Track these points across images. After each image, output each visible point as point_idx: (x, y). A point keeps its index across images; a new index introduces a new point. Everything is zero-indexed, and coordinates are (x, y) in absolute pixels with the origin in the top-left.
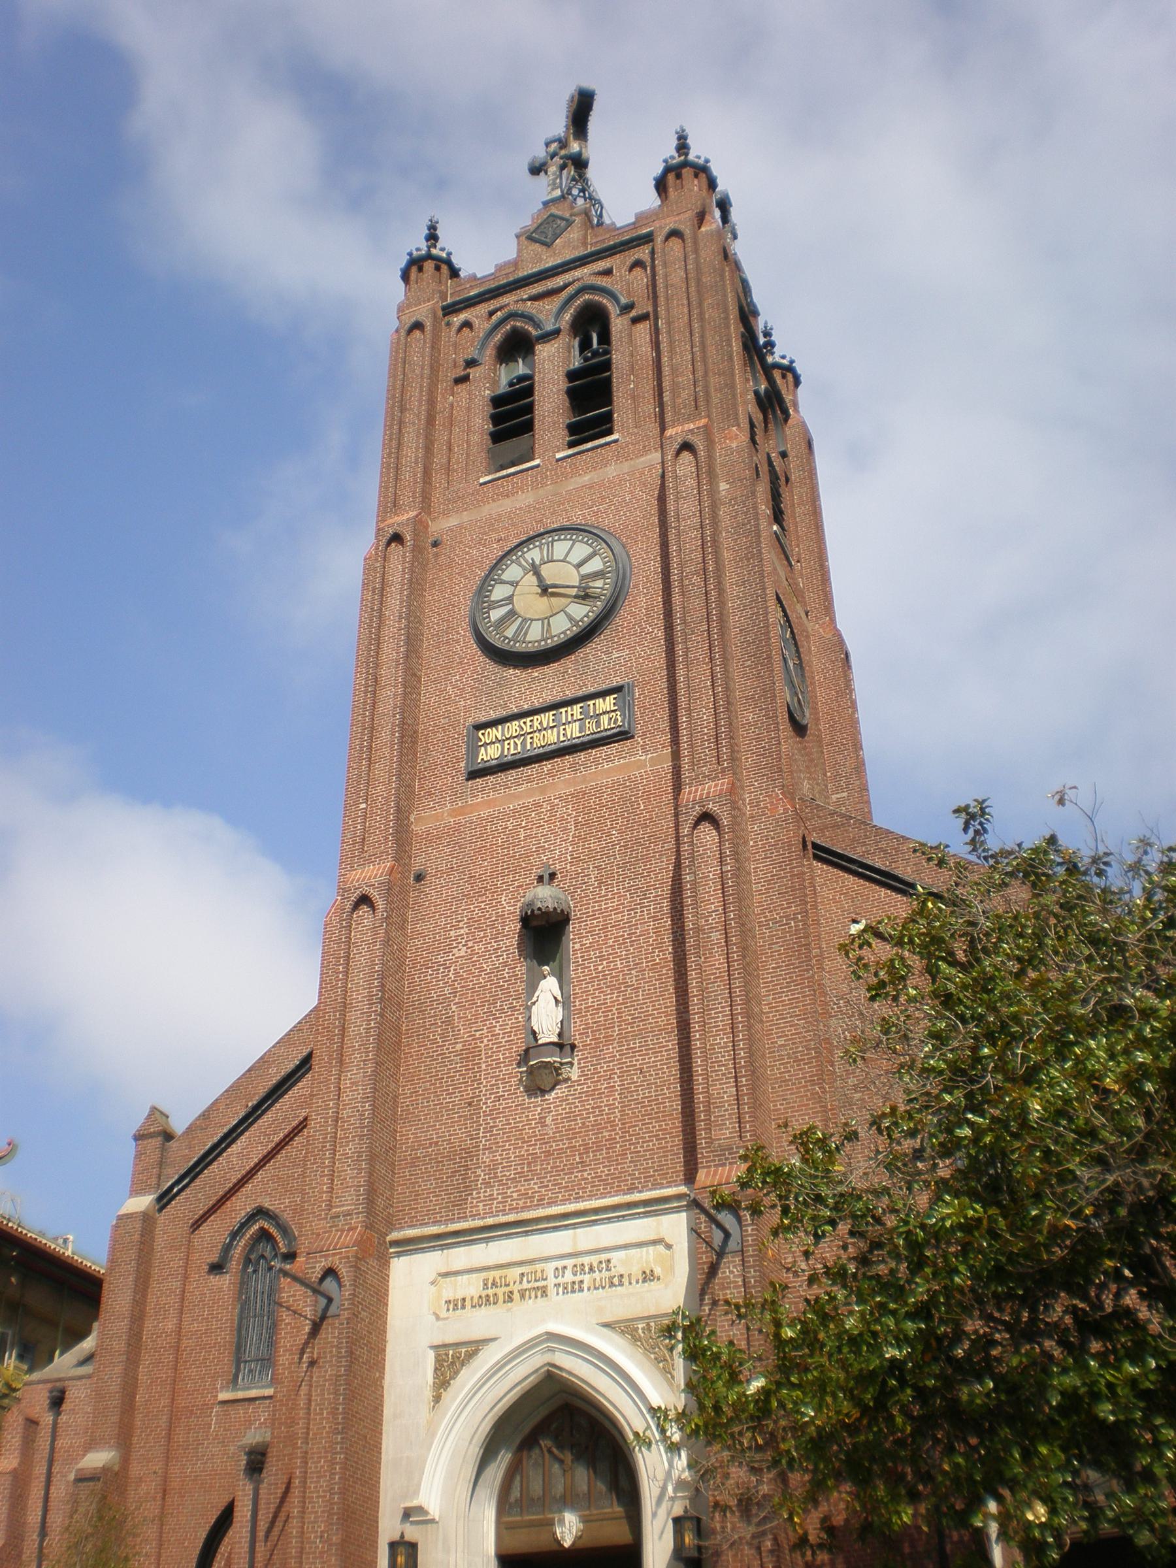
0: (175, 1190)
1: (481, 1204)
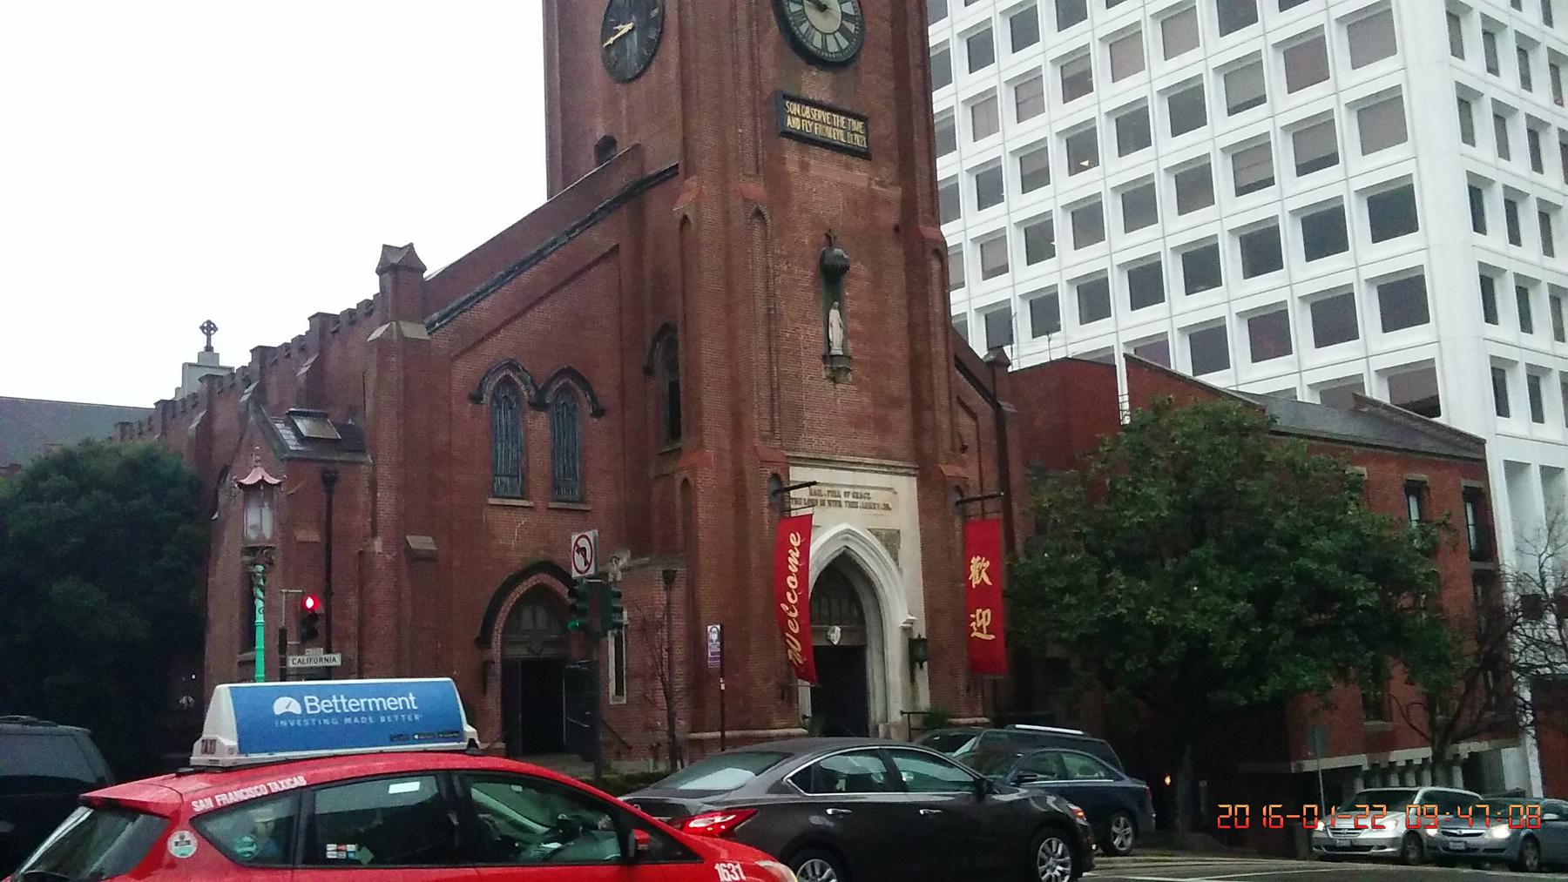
0: (437, 325)
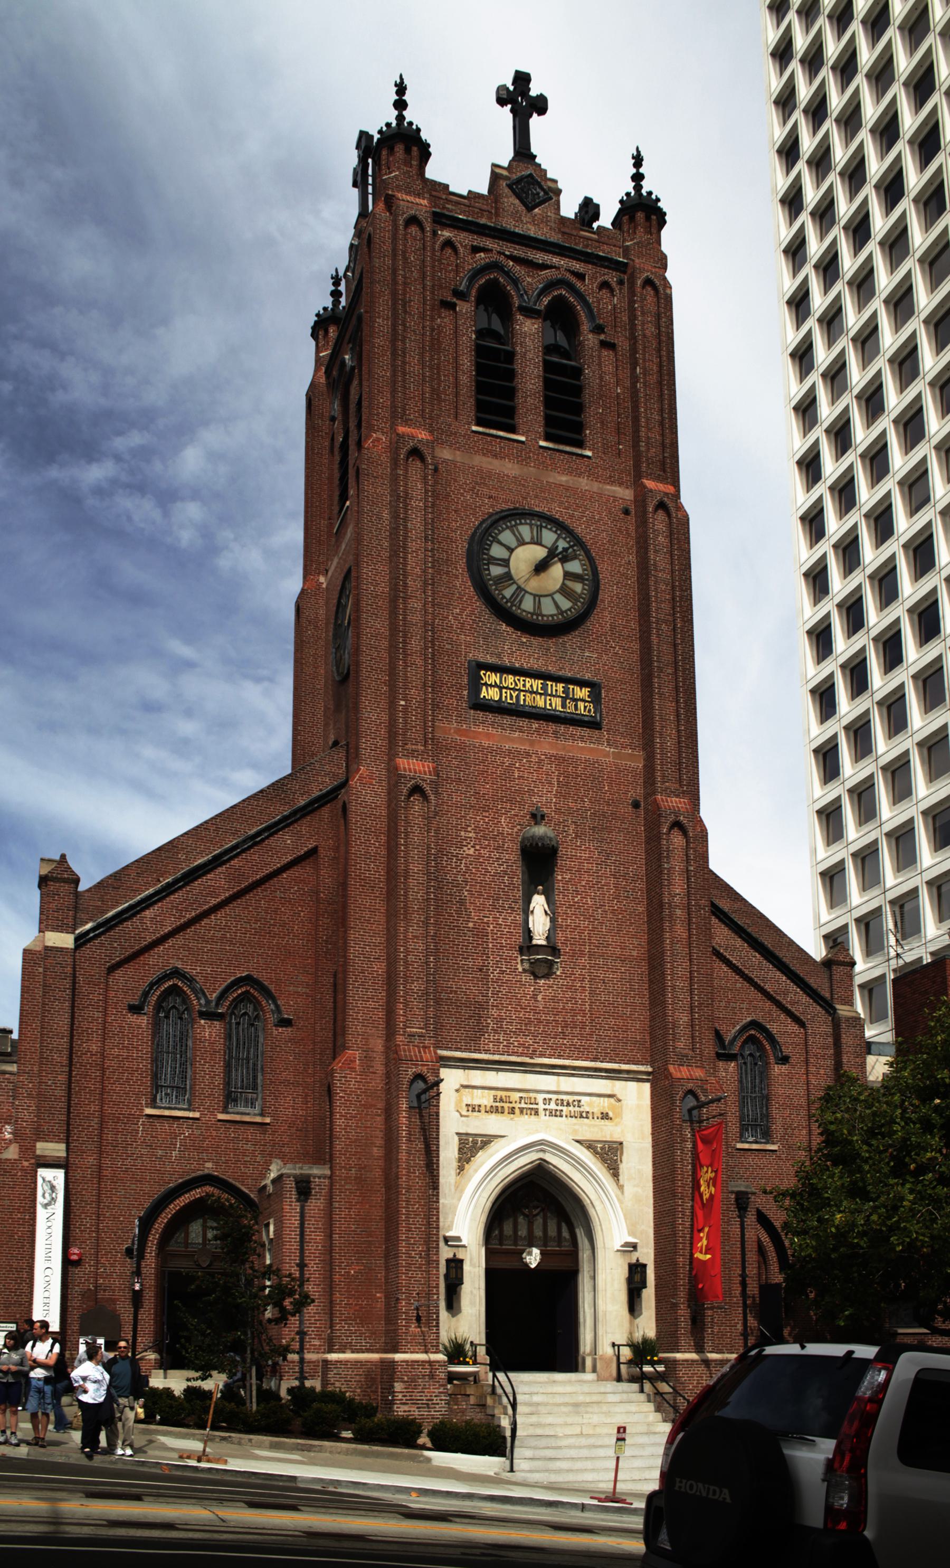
0: (91, 935)
1: (491, 1044)
